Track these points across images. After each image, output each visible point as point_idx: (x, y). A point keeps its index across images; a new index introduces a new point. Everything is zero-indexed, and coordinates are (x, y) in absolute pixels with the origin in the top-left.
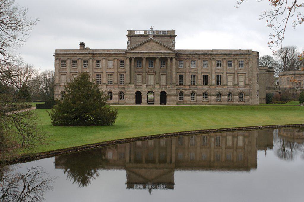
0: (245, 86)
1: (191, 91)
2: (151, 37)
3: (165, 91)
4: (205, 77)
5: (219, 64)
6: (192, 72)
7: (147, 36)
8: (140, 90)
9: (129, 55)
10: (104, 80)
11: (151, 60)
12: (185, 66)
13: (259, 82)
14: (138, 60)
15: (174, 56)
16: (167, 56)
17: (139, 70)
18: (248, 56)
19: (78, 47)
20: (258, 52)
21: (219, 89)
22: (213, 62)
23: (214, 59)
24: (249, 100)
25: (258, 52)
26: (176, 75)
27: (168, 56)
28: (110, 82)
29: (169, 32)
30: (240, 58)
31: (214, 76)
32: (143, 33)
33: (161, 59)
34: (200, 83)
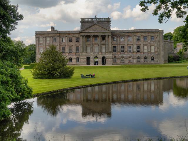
0: (155, 52)
1: (121, 56)
2: (95, 23)
3: (105, 56)
4: (130, 47)
5: (138, 39)
6: (121, 44)
7: (93, 22)
8: (89, 56)
9: (82, 34)
10: (67, 50)
11: (96, 37)
12: (117, 41)
13: (164, 50)
14: (88, 37)
15: (110, 34)
16: (106, 35)
17: (88, 43)
18: (157, 33)
19: (50, 30)
20: (163, 31)
21: (139, 54)
22: (135, 37)
23: (135, 35)
24: (157, 61)
25: (163, 31)
26: (112, 46)
27: (106, 34)
28: (70, 52)
29: (107, 19)
31: (135, 47)
32: (90, 20)
33: (102, 36)
34: (127, 51)
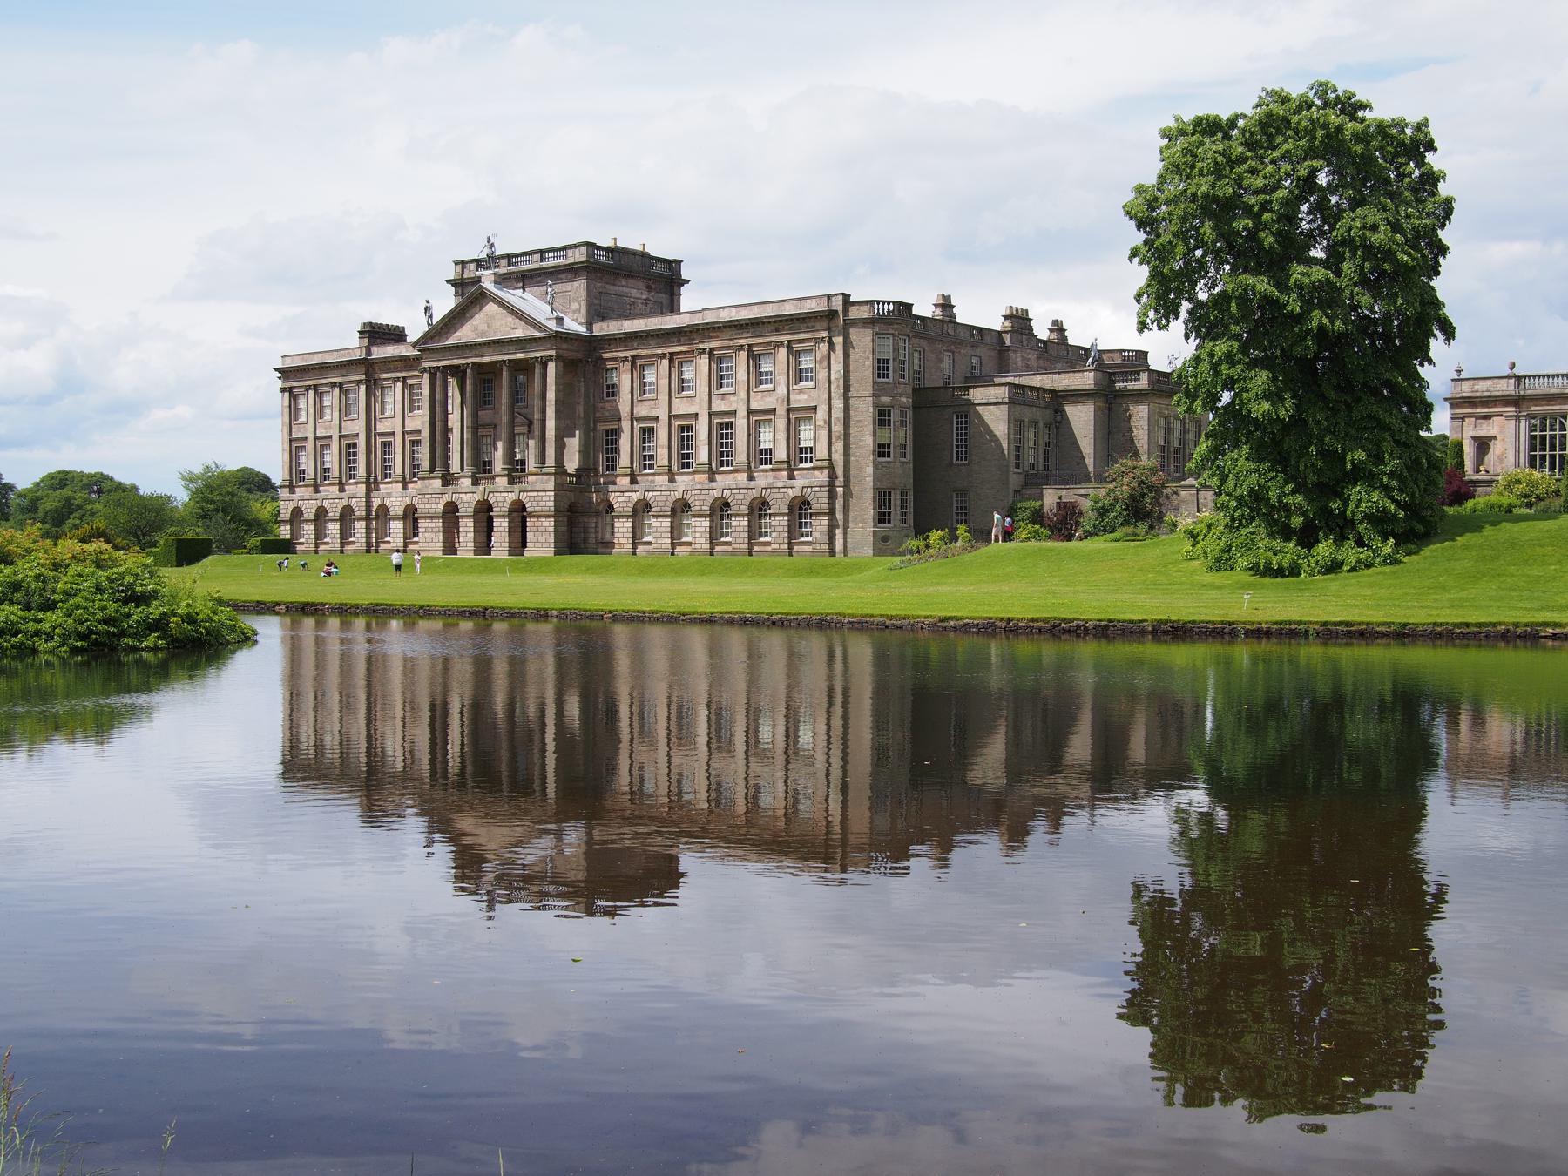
1: (635, 497)
3: (523, 496)
30: (796, 337)
